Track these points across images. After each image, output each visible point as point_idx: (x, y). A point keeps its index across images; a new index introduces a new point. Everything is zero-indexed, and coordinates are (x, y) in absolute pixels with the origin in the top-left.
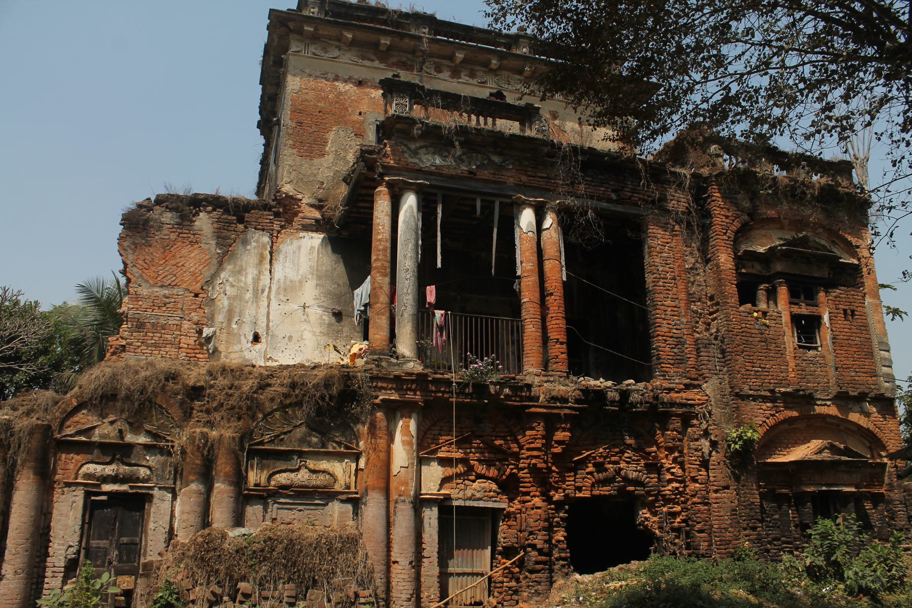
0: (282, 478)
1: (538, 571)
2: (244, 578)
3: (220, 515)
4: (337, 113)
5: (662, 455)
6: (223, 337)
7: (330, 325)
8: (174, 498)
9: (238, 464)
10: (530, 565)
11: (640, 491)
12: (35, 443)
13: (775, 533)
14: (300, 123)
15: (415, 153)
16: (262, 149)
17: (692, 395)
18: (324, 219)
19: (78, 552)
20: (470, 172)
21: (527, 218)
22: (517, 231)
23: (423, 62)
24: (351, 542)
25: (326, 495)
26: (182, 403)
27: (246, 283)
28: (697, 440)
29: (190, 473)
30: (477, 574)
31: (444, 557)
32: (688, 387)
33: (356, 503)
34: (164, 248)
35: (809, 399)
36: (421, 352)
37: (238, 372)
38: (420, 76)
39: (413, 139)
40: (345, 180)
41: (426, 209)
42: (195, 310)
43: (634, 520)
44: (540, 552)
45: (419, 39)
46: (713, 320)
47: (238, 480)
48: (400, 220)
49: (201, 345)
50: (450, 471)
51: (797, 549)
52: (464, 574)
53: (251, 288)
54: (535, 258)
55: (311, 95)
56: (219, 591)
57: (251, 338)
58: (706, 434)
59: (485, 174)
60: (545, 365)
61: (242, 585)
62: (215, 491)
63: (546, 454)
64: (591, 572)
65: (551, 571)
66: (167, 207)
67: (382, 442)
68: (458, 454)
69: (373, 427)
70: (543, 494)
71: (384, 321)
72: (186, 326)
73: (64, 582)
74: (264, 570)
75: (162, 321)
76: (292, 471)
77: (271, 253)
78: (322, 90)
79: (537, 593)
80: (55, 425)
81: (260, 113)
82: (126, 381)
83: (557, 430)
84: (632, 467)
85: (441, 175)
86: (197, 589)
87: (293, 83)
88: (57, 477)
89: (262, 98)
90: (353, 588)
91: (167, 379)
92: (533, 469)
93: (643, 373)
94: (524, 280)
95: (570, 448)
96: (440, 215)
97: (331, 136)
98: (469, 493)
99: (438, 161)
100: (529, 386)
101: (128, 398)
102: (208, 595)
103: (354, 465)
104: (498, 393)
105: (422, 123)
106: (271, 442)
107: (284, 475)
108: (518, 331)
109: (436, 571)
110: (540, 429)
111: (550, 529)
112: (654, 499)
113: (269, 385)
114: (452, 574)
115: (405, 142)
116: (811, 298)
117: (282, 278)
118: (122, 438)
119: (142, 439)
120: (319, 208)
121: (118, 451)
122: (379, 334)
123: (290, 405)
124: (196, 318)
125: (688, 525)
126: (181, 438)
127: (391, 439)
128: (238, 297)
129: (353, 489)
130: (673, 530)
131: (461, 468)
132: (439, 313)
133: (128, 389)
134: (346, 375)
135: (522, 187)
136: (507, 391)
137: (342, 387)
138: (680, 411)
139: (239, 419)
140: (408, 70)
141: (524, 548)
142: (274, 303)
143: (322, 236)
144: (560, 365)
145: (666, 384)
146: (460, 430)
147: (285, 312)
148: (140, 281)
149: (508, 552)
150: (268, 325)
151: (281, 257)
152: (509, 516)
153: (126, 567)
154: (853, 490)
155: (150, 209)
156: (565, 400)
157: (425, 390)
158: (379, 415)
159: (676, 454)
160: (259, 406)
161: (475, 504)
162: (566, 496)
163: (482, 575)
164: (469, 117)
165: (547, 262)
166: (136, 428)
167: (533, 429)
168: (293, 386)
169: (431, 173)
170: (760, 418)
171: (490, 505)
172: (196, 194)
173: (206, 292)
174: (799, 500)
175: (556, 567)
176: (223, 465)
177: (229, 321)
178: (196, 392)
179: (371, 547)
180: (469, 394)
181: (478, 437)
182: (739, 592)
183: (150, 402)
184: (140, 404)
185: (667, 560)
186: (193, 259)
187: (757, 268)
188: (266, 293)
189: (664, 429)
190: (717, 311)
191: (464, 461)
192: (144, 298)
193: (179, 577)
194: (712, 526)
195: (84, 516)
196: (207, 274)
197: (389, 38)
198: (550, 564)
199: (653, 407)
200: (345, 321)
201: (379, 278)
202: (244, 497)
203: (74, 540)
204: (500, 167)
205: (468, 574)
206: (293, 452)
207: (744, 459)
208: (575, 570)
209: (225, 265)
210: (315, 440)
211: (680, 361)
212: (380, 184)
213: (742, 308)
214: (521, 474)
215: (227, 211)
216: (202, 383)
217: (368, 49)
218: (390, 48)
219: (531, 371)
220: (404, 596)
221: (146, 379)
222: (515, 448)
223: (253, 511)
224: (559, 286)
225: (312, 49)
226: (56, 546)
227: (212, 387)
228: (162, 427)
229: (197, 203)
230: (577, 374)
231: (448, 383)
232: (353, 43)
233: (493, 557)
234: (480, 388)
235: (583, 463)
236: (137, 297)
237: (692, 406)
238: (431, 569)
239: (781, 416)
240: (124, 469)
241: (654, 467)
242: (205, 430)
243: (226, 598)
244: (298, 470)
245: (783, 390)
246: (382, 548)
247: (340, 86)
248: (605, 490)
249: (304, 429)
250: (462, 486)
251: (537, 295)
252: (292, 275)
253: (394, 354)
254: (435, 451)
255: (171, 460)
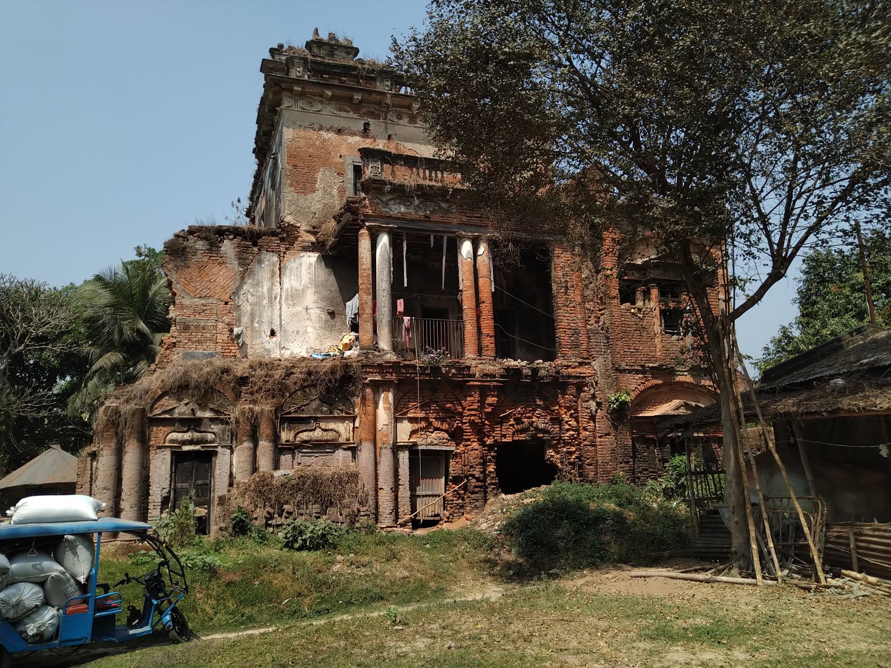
0: (304, 436)
1: (476, 493)
2: (287, 502)
3: (265, 463)
4: (322, 157)
5: (562, 412)
6: (249, 333)
7: (326, 321)
8: (232, 452)
9: (275, 428)
10: (471, 489)
11: (547, 437)
12: (136, 422)
13: (645, 466)
14: (295, 166)
15: (386, 204)
16: (256, 167)
17: (585, 370)
18: (318, 243)
19: (170, 492)
20: (426, 217)
21: (466, 248)
22: (459, 257)
23: (387, 112)
24: (354, 477)
25: (332, 445)
26: (234, 389)
27: (262, 293)
28: (587, 401)
29: (243, 436)
30: (436, 496)
31: (414, 485)
32: (581, 364)
33: (354, 451)
34: (199, 268)
35: (672, 372)
36: (395, 347)
37: (269, 366)
38: (386, 123)
39: (383, 194)
40: (334, 217)
41: (395, 244)
42: (226, 314)
43: (544, 457)
44: (478, 479)
45: (384, 94)
46: (602, 315)
47: (275, 438)
48: (377, 253)
49: (232, 340)
50: (416, 426)
51: (660, 477)
52: (427, 496)
53: (266, 297)
54: (472, 277)
55: (302, 143)
56: (272, 511)
57: (269, 333)
58: (594, 397)
59: (436, 217)
60: (480, 351)
61: (286, 507)
62: (260, 447)
63: (481, 413)
64: (513, 492)
65: (485, 492)
66: (199, 237)
67: (370, 409)
68: (421, 415)
69: (364, 399)
70: (479, 440)
71: (369, 326)
72: (220, 327)
73: (161, 512)
74: (299, 497)
75: (202, 324)
76: (311, 431)
77: (280, 269)
78: (310, 138)
79: (476, 507)
80: (148, 408)
81: (256, 143)
82: (195, 376)
83: (488, 396)
84: (541, 420)
85: (405, 219)
86: (258, 510)
87: (288, 134)
88: (151, 443)
89: (258, 133)
90: (356, 506)
91: (222, 373)
92: (472, 423)
93: (550, 357)
94: (464, 293)
95: (497, 408)
96: (405, 249)
97: (319, 176)
98: (429, 441)
99: (403, 209)
100: (469, 367)
101: (196, 387)
102: (265, 514)
103: (352, 425)
104: (448, 372)
105: (391, 184)
106: (296, 412)
107: (305, 433)
108: (461, 330)
109: (408, 494)
110: (477, 396)
111: (484, 464)
112: (557, 443)
113: (293, 373)
114: (419, 496)
115: (379, 196)
116: (676, 296)
117: (290, 288)
118: (194, 414)
119: (208, 414)
120: (315, 233)
121: (193, 423)
122: (366, 334)
123: (308, 386)
124: (227, 321)
125: (580, 460)
126: (235, 412)
127: (376, 406)
128: (258, 304)
129: (351, 441)
130: (570, 463)
131: (423, 424)
132: (406, 319)
133: (197, 381)
134: (347, 367)
135: (462, 225)
136: (453, 371)
137: (342, 374)
138: (575, 381)
139: (273, 397)
140: (376, 118)
141: (467, 477)
142: (284, 307)
143: (317, 255)
144: (490, 352)
145: (565, 363)
146: (422, 398)
147: (291, 316)
148: (183, 294)
149: (456, 480)
150: (281, 323)
151: (288, 272)
152: (456, 455)
153: (202, 499)
154: (702, 435)
155: (185, 238)
156: (494, 376)
157: (398, 372)
158: (368, 390)
159: (572, 411)
160: (287, 388)
161: (433, 448)
162: (495, 441)
163: (439, 496)
164: (424, 172)
165: (480, 279)
166: (203, 407)
167: (472, 396)
168: (309, 373)
169: (398, 219)
170: (634, 384)
171: (444, 448)
172: (220, 226)
173: (233, 300)
174: (661, 443)
175: (489, 490)
176: (265, 429)
177: (252, 321)
178: (243, 381)
179: (366, 479)
180: (428, 374)
181: (435, 402)
182: (610, 506)
183: (212, 389)
184: (204, 390)
185: (566, 485)
186: (222, 276)
187: (636, 276)
188: (278, 299)
189: (564, 394)
190: (604, 309)
191: (426, 419)
192: (187, 307)
193: (246, 503)
194: (597, 461)
195: (171, 468)
196: (234, 287)
197: (361, 94)
198: (486, 487)
199: (555, 379)
200: (338, 318)
201: (365, 297)
202: (279, 450)
203: (166, 484)
204: (448, 211)
205: (430, 496)
206: (311, 418)
207: (620, 414)
208: (502, 492)
209: (246, 280)
210: (325, 409)
211: (576, 346)
212: (361, 228)
213: (623, 307)
214: (464, 427)
215: (245, 239)
216: (247, 374)
217: (344, 102)
218: (361, 101)
219: (470, 356)
220: (388, 511)
221: (208, 373)
222: (460, 409)
223: (285, 459)
224: (489, 296)
225: (300, 104)
226: (154, 489)
227: (253, 376)
228: (220, 405)
229: (221, 232)
230: (503, 358)
231: (414, 367)
232: (333, 98)
233: (446, 484)
234: (436, 370)
235: (507, 418)
236: (182, 307)
237: (584, 377)
238: (404, 493)
239: (648, 384)
240: (197, 435)
241: (557, 420)
242: (251, 406)
243: (276, 516)
244: (314, 430)
245: (651, 365)
246: (372, 478)
247: (325, 135)
248: (522, 437)
249: (317, 402)
250: (425, 436)
251: (474, 303)
252: (296, 284)
253: (376, 348)
254: (406, 413)
255: (228, 427)
